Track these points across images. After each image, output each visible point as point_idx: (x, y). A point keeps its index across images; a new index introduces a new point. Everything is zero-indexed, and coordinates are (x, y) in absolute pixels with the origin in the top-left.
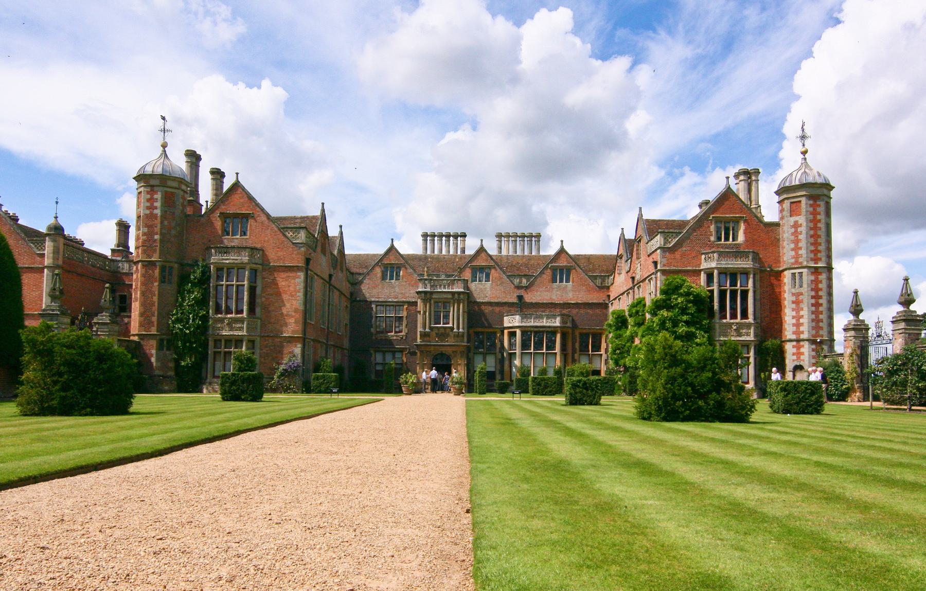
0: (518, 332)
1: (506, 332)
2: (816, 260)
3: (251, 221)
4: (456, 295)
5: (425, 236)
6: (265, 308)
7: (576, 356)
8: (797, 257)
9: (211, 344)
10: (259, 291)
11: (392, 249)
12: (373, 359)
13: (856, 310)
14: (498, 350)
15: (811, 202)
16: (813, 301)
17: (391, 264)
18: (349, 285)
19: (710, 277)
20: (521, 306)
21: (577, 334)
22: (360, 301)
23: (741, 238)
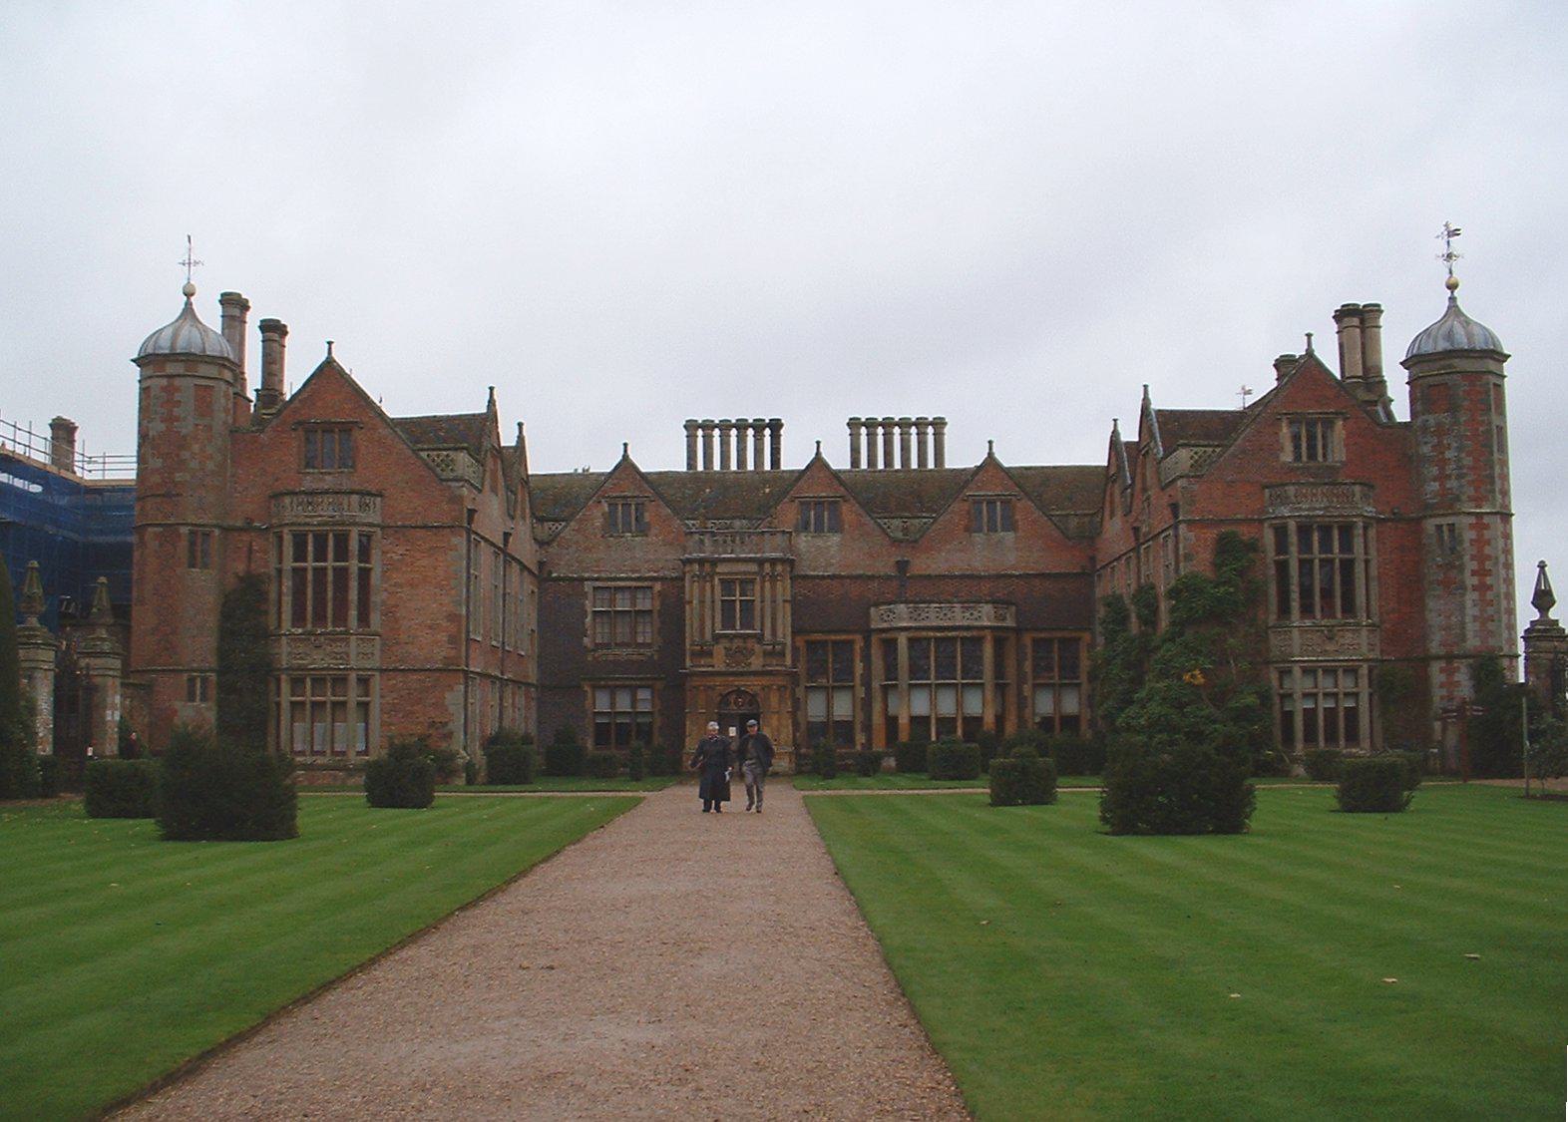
0: (902, 640)
1: (874, 639)
2: (1478, 501)
3: (356, 433)
4: (767, 566)
5: (691, 427)
6: (389, 613)
7: (1027, 689)
9: (285, 687)
10: (375, 578)
11: (626, 465)
12: (589, 701)
13: (1543, 598)
14: (858, 680)
17: (626, 490)
18: (536, 547)
19: (1281, 532)
20: (904, 584)
21: (1027, 639)
22: (558, 579)
23: (1338, 454)
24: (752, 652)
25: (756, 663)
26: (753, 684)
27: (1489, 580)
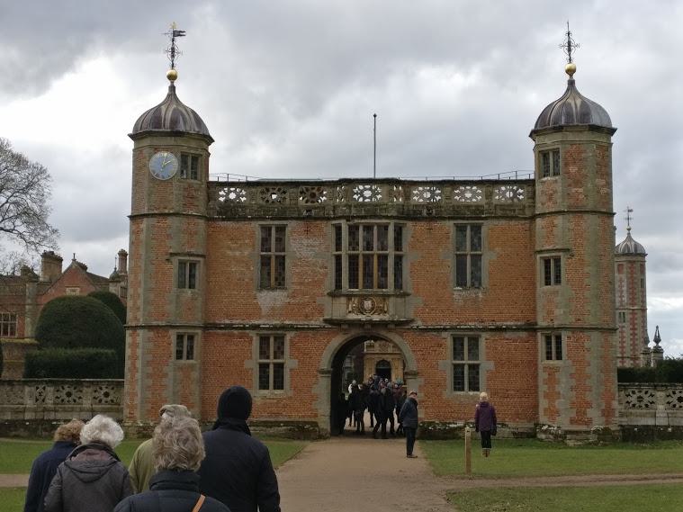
2: (633, 305)
8: (622, 301)
15: (630, 265)
16: (631, 332)
24: (389, 346)
25: (390, 350)
26: (389, 358)
27: (636, 332)
